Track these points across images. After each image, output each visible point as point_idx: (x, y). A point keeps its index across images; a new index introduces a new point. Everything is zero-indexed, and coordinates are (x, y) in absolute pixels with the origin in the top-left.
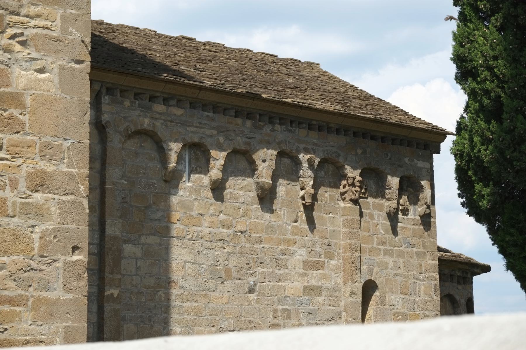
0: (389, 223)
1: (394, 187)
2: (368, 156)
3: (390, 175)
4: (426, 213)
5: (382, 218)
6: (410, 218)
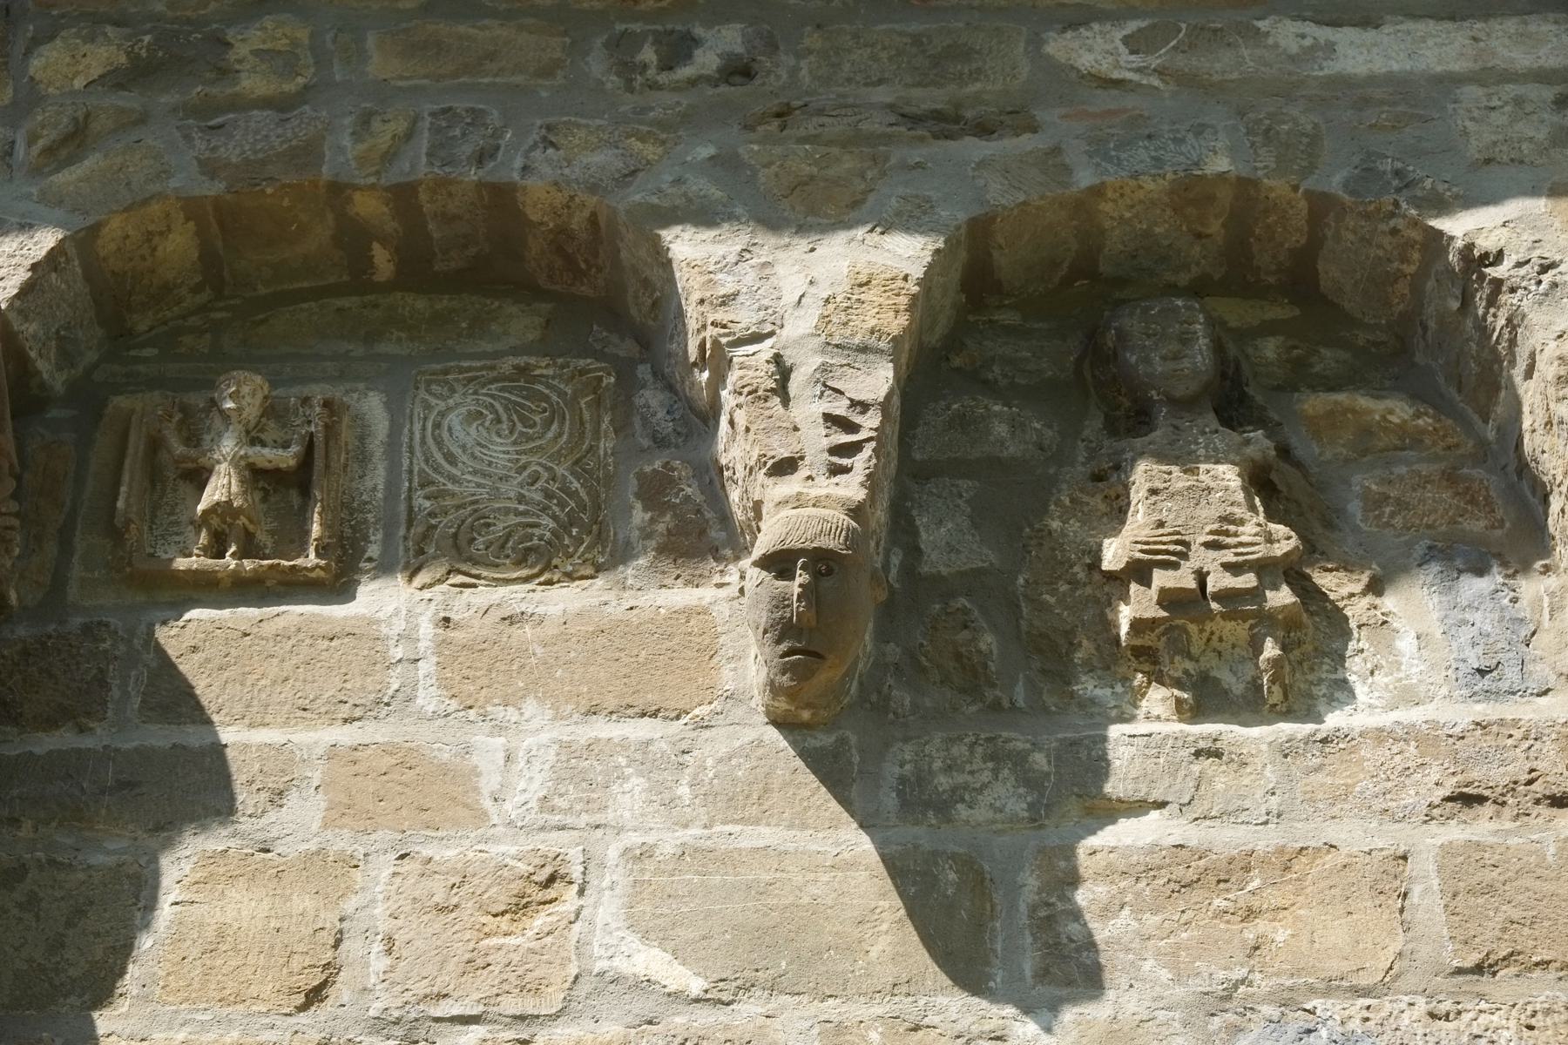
0: (864, 845)
1: (798, 327)
2: (253, 83)
3: (704, 216)
6: (1380, 736)
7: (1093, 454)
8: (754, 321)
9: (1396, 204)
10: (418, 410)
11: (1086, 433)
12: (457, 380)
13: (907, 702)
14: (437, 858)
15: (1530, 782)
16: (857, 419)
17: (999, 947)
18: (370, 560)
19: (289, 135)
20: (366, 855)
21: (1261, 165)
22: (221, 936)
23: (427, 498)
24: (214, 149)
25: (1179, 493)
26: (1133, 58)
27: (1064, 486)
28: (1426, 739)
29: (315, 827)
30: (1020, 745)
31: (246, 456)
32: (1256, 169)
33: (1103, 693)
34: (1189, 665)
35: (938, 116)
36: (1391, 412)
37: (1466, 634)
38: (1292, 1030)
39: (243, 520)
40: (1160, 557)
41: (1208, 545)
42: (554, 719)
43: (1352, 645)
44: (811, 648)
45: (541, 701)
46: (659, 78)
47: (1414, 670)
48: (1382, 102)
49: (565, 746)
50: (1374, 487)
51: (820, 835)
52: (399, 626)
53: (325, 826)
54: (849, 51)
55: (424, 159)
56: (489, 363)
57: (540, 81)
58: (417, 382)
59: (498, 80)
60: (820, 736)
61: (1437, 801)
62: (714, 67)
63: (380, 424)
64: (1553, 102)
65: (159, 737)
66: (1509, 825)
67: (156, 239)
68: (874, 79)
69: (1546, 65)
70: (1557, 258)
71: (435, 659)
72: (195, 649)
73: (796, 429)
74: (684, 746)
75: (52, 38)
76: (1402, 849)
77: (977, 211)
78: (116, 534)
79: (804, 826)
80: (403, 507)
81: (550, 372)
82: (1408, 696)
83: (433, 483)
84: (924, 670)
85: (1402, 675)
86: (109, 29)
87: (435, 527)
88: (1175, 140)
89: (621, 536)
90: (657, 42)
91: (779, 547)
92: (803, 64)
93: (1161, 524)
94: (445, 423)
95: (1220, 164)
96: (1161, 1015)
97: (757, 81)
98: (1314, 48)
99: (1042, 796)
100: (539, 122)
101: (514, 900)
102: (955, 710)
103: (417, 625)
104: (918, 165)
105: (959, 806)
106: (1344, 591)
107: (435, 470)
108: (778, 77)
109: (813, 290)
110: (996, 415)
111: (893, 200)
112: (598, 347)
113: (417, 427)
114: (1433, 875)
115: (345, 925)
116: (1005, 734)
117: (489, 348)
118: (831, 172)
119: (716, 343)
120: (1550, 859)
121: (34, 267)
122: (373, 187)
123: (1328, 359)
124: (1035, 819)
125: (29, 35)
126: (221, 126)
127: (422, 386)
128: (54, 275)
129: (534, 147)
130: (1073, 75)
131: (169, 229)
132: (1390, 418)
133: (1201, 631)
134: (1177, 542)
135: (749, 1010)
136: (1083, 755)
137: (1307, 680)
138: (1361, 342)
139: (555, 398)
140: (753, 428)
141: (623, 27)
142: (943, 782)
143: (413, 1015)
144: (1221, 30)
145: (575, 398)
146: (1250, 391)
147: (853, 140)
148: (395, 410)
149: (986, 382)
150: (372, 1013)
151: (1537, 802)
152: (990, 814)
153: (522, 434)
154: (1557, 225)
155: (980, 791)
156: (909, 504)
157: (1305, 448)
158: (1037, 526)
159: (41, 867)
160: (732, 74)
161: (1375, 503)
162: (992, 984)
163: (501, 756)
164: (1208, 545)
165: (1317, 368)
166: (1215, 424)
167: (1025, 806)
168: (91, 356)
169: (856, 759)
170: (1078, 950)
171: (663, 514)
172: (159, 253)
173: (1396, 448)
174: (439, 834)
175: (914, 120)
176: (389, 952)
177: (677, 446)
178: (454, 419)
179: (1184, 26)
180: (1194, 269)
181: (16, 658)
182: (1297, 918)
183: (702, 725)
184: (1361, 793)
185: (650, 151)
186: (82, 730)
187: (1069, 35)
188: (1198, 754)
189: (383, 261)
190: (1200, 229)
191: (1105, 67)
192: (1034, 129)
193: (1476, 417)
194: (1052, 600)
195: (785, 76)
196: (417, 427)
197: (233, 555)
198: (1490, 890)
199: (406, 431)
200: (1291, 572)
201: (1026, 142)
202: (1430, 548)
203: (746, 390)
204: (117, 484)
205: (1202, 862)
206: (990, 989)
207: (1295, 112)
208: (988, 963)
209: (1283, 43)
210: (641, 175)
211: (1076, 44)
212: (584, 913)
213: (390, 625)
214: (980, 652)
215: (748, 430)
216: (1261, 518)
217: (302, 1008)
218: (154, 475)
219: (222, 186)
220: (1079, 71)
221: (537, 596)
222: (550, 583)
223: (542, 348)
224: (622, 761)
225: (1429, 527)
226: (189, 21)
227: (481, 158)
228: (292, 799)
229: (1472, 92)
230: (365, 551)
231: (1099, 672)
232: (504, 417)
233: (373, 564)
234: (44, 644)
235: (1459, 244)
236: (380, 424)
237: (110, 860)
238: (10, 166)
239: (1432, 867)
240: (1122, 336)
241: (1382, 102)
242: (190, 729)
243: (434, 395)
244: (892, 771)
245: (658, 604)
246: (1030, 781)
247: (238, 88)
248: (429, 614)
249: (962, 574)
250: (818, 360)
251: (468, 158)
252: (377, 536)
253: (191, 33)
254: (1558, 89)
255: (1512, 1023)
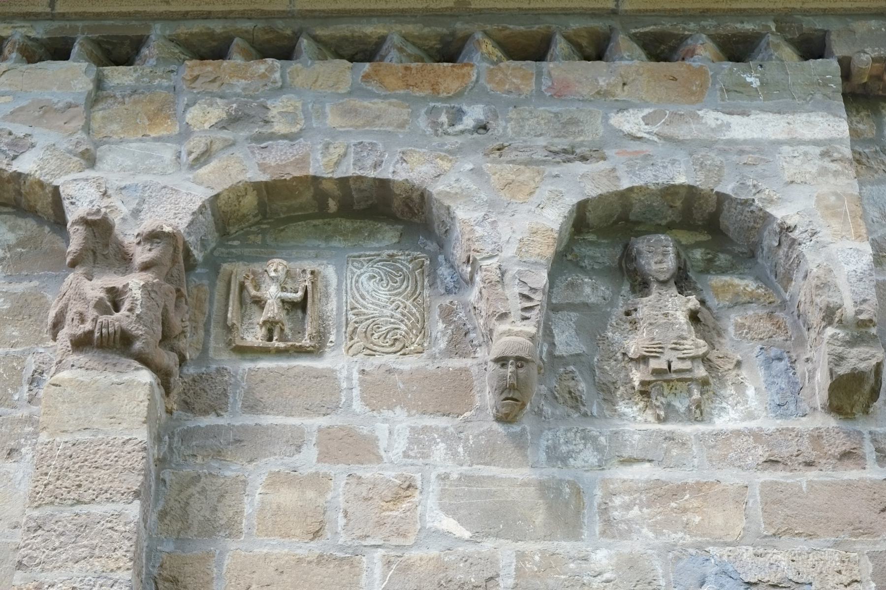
1: (509, 252)
2: (279, 127)
4: (842, 370)
5: (449, 448)
6: (738, 433)
7: (626, 303)
8: (490, 249)
9: (753, 200)
10: (349, 274)
11: (623, 292)
12: (364, 260)
13: (550, 412)
14: (363, 477)
15: (797, 455)
16: (532, 296)
17: (586, 521)
18: (331, 342)
19: (295, 153)
20: (335, 474)
21: (697, 179)
22: (279, 507)
23: (354, 315)
24: (264, 159)
25: (660, 325)
26: (646, 127)
27: (614, 317)
28: (757, 436)
29: (315, 461)
30: (595, 433)
31: (280, 297)
32: (696, 181)
33: (628, 410)
34: (663, 400)
35: (565, 151)
36: (747, 286)
37: (774, 389)
38: (700, 560)
39: (280, 324)
40: (652, 354)
41: (672, 349)
42: (408, 416)
43: (728, 392)
44: (514, 397)
45: (402, 408)
46: (448, 130)
47: (753, 404)
48: (749, 153)
49: (413, 429)
50: (739, 320)
51: (515, 471)
52: (345, 373)
53: (319, 461)
54: (528, 120)
55: (352, 167)
56: (377, 253)
57: (399, 130)
58: (348, 261)
59: (381, 129)
60: (515, 426)
61: (760, 463)
62: (472, 126)
63: (333, 281)
64: (820, 155)
65: (249, 420)
66: (789, 474)
67: (241, 199)
68: (539, 133)
69: (817, 138)
70: (818, 230)
71: (359, 388)
72: (262, 381)
73: (507, 299)
74: (460, 429)
75: (195, 103)
76: (746, 483)
77: (581, 198)
78: (229, 329)
79: (510, 467)
80: (344, 319)
81: (402, 258)
82: (750, 416)
83: (356, 308)
84: (556, 398)
85: (748, 406)
86: (218, 100)
87: (357, 328)
88: (663, 166)
89: (433, 335)
90: (447, 112)
91: (502, 355)
92: (509, 125)
93: (653, 339)
94: (360, 280)
95: (681, 179)
96: (649, 552)
97: (490, 133)
98: (721, 125)
99: (603, 456)
100: (399, 150)
101: (395, 496)
102: (569, 416)
103: (352, 373)
104: (557, 176)
105: (570, 459)
106: (726, 368)
107: (357, 302)
108: (499, 131)
109: (514, 235)
110: (586, 283)
111: (547, 192)
112: (422, 246)
113: (349, 281)
114: (758, 495)
115: (327, 505)
116: (589, 428)
117: (377, 245)
118: (521, 178)
119: (475, 260)
120: (804, 489)
121: (194, 213)
122: (330, 178)
123: (723, 259)
124: (601, 467)
125: (185, 102)
126: (266, 147)
127: (350, 263)
128: (200, 216)
129: (397, 162)
130: (621, 134)
131: (246, 194)
132: (747, 288)
133: (668, 385)
134: (660, 348)
135: (488, 545)
136: (620, 438)
137: (710, 407)
138: (736, 252)
139: (405, 269)
140: (491, 298)
141: (433, 104)
142: (564, 449)
143: (356, 544)
144: (683, 115)
145: (414, 270)
146: (690, 274)
147: (528, 163)
148: (339, 273)
149: (582, 267)
150: (339, 543)
151: (800, 464)
152: (583, 463)
153: (392, 286)
154: (819, 214)
155: (578, 453)
156: (550, 323)
157: (712, 302)
158: (603, 335)
159: (206, 476)
160: (479, 128)
161: (739, 327)
162: (583, 537)
163: (387, 432)
164: (672, 349)
165: (718, 263)
166: (676, 293)
167: (596, 460)
168: (213, 245)
169: (529, 437)
170: (617, 523)
171: (450, 325)
172: (242, 203)
173: (749, 302)
174: (364, 466)
175: (556, 153)
176: (346, 517)
177: (455, 293)
178: (363, 278)
179: (668, 112)
180: (668, 219)
181: (191, 383)
182: (704, 512)
183: (466, 421)
184: (731, 458)
185: (446, 165)
186: (218, 415)
187: (620, 114)
188: (666, 439)
189: (332, 206)
190: (672, 204)
191: (635, 131)
192: (604, 159)
193: (782, 289)
194: (608, 368)
195: (501, 131)
196: (349, 281)
197: (276, 340)
198: (780, 502)
199: (344, 283)
200: (704, 359)
201: (602, 165)
202: (761, 349)
203: (487, 281)
204: (227, 305)
205: (667, 487)
206: (582, 539)
207: (713, 155)
208: (581, 528)
209: (709, 122)
210: (442, 176)
211: (622, 120)
212: (422, 502)
213: (340, 373)
214: (578, 390)
215: (488, 299)
216: (694, 337)
217: (312, 540)
218: (242, 302)
219: (269, 176)
220: (623, 132)
221: (400, 360)
222: (404, 354)
223: (399, 245)
224: (436, 436)
225: (761, 339)
226: (251, 97)
227: (376, 166)
228: (304, 449)
229: (786, 149)
230: (329, 338)
231: (627, 401)
232: (384, 278)
233: (333, 344)
234: (201, 377)
235: (779, 221)
236: (333, 281)
237: (233, 474)
238: (179, 163)
239: (758, 492)
240: (639, 253)
241: (749, 153)
242: (262, 416)
243: (355, 267)
244: (544, 443)
245: (449, 365)
246: (599, 449)
247: (273, 130)
248: (356, 368)
249: (572, 356)
250: (517, 268)
251: (371, 166)
252: (334, 331)
253: (252, 102)
254: (822, 149)
255: (786, 559)
